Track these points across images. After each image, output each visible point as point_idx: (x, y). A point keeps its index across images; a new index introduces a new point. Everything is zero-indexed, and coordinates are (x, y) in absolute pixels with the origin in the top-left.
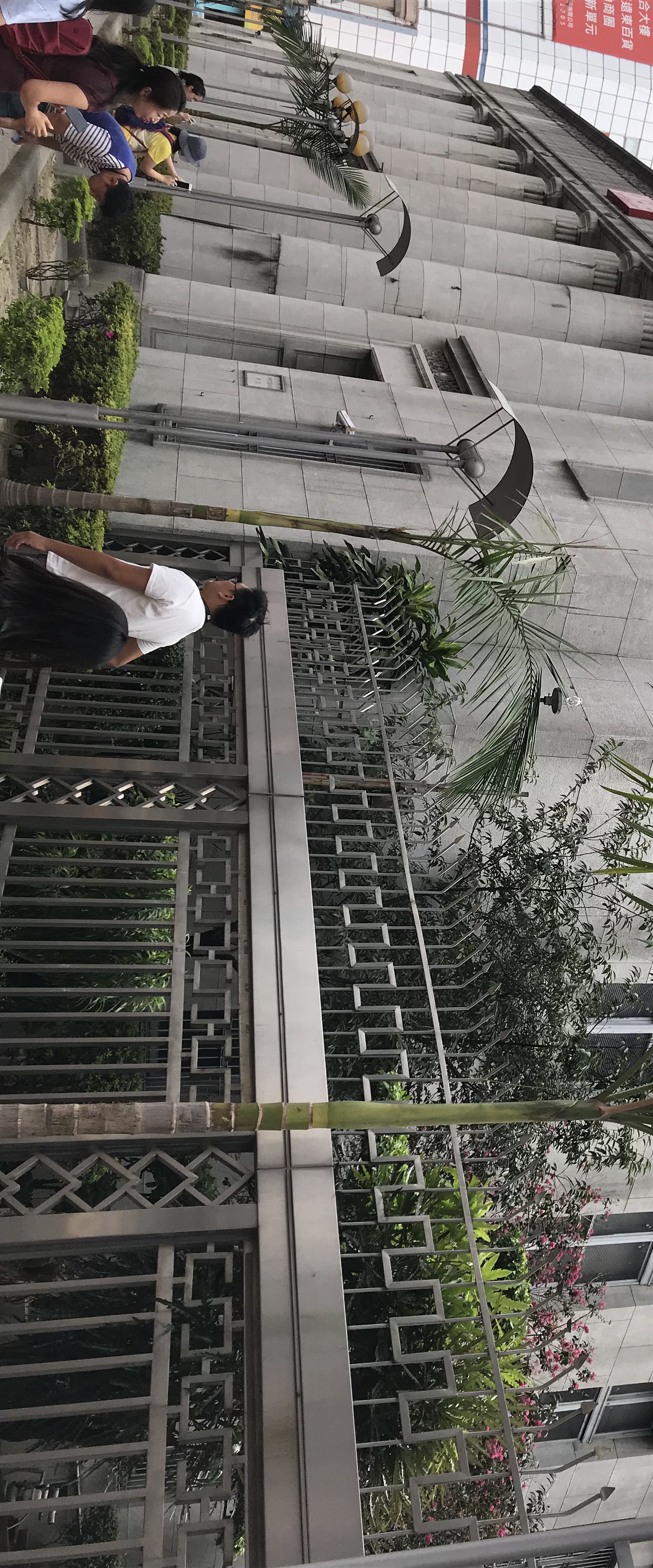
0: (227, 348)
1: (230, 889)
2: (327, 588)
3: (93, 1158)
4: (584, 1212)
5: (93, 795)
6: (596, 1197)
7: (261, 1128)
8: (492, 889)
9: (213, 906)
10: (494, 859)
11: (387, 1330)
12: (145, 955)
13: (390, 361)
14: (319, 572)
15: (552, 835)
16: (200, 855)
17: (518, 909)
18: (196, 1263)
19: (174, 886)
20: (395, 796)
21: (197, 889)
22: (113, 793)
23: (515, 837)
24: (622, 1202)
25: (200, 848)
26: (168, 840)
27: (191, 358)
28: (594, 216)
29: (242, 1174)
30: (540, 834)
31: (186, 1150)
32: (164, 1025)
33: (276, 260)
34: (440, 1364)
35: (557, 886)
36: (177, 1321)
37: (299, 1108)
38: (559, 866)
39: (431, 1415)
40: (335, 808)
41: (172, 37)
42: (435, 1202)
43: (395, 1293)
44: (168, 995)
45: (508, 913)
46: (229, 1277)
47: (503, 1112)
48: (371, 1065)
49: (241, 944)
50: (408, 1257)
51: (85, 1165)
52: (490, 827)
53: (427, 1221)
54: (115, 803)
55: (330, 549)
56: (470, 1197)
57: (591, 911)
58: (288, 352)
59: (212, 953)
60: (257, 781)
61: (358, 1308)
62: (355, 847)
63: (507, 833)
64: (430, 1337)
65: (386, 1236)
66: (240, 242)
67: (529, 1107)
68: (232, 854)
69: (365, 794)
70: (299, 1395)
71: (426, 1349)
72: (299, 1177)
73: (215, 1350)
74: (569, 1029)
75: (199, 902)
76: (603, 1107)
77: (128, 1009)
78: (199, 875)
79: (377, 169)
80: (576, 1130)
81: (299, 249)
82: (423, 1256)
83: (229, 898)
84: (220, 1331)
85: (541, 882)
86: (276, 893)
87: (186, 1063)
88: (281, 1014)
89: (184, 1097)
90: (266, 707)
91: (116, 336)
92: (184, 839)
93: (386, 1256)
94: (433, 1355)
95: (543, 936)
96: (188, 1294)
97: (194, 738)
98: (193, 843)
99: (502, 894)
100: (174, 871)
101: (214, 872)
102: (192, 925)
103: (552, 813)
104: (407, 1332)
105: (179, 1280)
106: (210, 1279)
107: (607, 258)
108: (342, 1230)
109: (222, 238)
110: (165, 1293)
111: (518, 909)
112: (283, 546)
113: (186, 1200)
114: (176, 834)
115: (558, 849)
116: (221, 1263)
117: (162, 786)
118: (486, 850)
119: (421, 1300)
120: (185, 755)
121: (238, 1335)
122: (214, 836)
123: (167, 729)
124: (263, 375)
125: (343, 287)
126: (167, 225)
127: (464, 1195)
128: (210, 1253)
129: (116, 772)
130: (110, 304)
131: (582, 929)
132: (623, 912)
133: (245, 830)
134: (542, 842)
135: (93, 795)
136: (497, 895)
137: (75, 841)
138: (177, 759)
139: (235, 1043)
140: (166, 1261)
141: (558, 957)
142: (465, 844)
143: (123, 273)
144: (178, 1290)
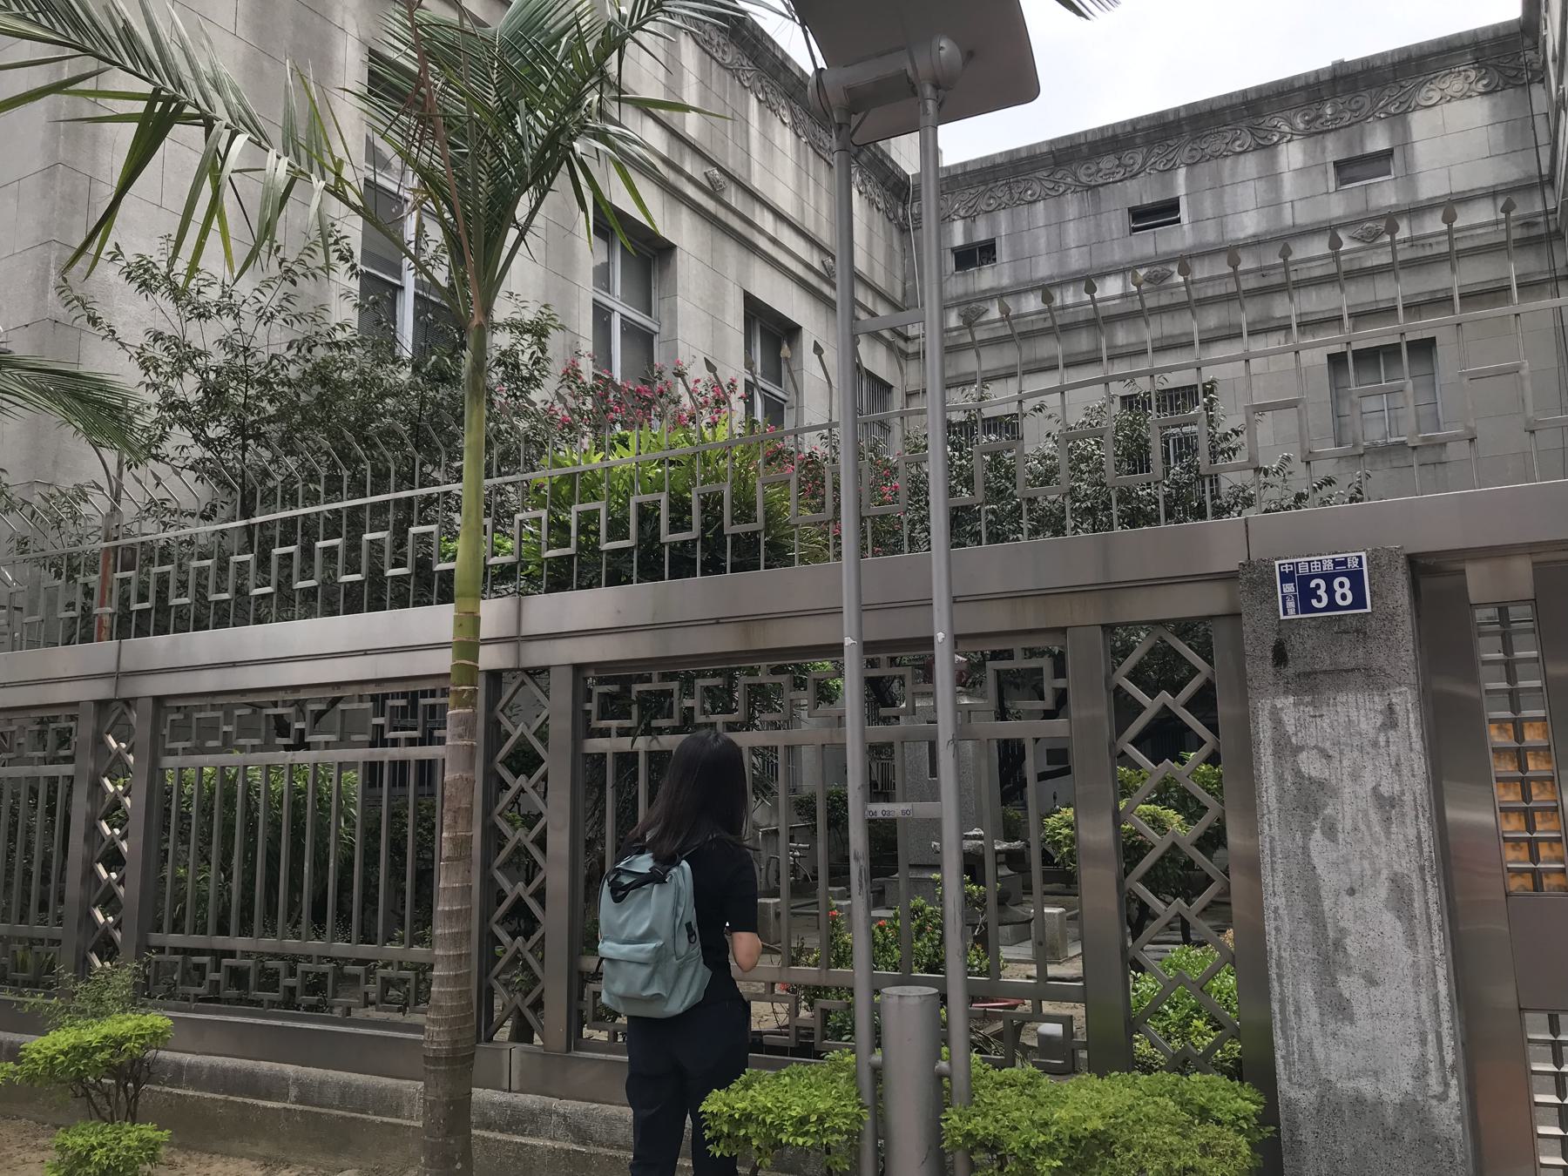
1: (228, 710)
3: (498, 820)
4: (588, 378)
5: (114, 859)
6: (574, 365)
7: (476, 660)
8: (244, 448)
9: (246, 730)
10: (208, 444)
12: (300, 792)
15: (181, 376)
16: (188, 744)
17: (270, 420)
18: (601, 718)
20: (121, 542)
21: (227, 746)
22: (113, 842)
23: (180, 419)
24: (582, 341)
25: (180, 745)
29: (523, 683)
30: (178, 390)
31: (495, 734)
32: (373, 769)
35: (243, 376)
36: (649, 731)
37: (459, 625)
38: (218, 372)
40: (135, 607)
42: (559, 499)
43: (640, 540)
45: (274, 431)
46: (614, 688)
47: (474, 424)
48: (423, 565)
51: (504, 826)
52: (168, 448)
53: (577, 508)
54: (124, 837)
56: (560, 466)
57: (272, 340)
60: (102, 690)
61: (650, 571)
62: (183, 585)
63: (176, 427)
64: (680, 509)
65: (589, 548)
67: (471, 398)
70: (718, 621)
72: (528, 629)
74: (405, 375)
75: (242, 742)
76: (475, 322)
77: (354, 805)
78: (211, 744)
80: (508, 378)
83: (238, 712)
85: (237, 393)
86: (234, 664)
87: (411, 742)
88: (365, 653)
89: (441, 741)
92: (169, 762)
93: (605, 546)
95: (298, 396)
96: (627, 723)
97: (45, 761)
98: (173, 752)
99: (250, 437)
100: (206, 770)
101: (211, 728)
102: (267, 746)
104: (673, 529)
105: (613, 732)
106: (614, 706)
108: (580, 587)
110: (625, 744)
111: (270, 420)
115: (197, 371)
117: (105, 791)
118: (197, 452)
119: (647, 515)
120: (68, 769)
121: (665, 677)
122: (166, 732)
123: (34, 793)
127: (557, 473)
128: (592, 707)
129: (86, 839)
131: (294, 351)
132: (275, 303)
133: (159, 700)
134: (188, 388)
135: (114, 859)
136: (251, 441)
138: (71, 778)
139: (395, 696)
140: (596, 745)
141: (324, 381)
142: (189, 476)
144: (623, 732)
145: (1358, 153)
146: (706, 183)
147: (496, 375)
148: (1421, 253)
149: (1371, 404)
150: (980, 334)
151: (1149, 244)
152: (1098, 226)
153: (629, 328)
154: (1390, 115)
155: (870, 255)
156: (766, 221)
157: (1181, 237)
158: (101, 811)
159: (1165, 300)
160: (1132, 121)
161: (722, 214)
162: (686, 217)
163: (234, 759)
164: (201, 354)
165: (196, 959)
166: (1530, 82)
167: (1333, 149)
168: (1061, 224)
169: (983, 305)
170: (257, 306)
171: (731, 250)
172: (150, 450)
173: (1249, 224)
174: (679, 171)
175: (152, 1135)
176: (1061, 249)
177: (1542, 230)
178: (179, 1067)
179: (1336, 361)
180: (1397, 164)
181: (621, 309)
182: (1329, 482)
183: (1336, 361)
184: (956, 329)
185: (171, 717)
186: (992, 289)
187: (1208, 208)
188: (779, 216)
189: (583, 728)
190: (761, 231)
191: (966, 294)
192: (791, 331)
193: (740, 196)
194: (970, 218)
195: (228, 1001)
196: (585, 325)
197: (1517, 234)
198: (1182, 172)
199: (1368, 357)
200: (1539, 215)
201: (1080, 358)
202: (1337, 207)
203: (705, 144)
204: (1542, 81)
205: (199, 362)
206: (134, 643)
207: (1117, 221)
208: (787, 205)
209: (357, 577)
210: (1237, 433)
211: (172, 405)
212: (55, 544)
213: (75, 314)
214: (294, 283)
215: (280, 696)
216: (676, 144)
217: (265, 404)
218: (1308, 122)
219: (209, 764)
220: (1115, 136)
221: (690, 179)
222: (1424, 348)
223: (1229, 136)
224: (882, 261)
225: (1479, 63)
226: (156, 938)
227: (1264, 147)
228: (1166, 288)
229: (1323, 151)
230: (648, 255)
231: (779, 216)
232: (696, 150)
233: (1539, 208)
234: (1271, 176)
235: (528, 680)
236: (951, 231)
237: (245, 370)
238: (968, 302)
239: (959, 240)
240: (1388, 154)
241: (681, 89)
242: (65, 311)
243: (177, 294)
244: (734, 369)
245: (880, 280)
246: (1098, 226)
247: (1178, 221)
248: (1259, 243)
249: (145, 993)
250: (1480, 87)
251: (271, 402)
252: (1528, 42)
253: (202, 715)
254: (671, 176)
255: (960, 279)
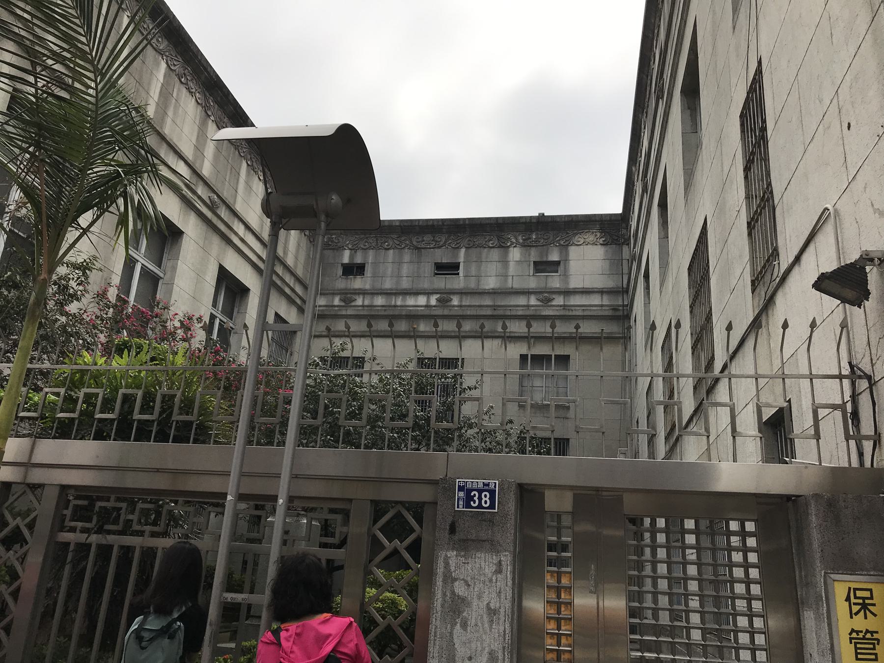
11: (139, 421)
18: (72, 520)
29: (25, 492)
34: (164, 396)
36: (100, 530)
39: (187, 406)
43: (120, 414)
46: (85, 503)
50: (103, 403)
61: (123, 434)
65: (88, 415)
70: (158, 470)
71: (154, 402)
72: (36, 459)
73: (123, 512)
82: (104, 395)
84: (114, 509)
93: (98, 416)
94: (158, 399)
96: (87, 525)
106: (82, 514)
110: (82, 538)
113: (31, 526)
116: (76, 506)
121: (118, 500)
128: (68, 512)
144: (84, 531)
145: (545, 259)
146: (208, 202)
147: (52, 289)
148: (567, 313)
149: (537, 383)
150: (350, 312)
151: (441, 282)
152: (418, 268)
153: (145, 271)
154: (560, 245)
155: (296, 258)
156: (240, 229)
157: (459, 282)
159: (446, 312)
160: (442, 220)
161: (215, 220)
162: (193, 218)
166: (623, 244)
167: (534, 255)
168: (400, 263)
169: (354, 297)
171: (216, 240)
173: (491, 283)
174: (194, 192)
176: (399, 276)
177: (621, 313)
179: (523, 357)
180: (561, 268)
181: (142, 260)
182: (511, 422)
183: (523, 357)
184: (338, 306)
186: (360, 289)
187: (473, 271)
188: (248, 227)
189: (59, 524)
190: (236, 234)
191: (346, 289)
192: (244, 291)
193: (227, 213)
194: (354, 250)
196: (118, 267)
197: (610, 313)
198: (463, 250)
199: (540, 360)
200: (620, 306)
201: (400, 334)
202: (532, 283)
203: (212, 182)
204: (628, 244)
207: (428, 268)
208: (254, 223)
210: (470, 389)
216: (194, 180)
218: (524, 240)
220: (433, 226)
221: (199, 197)
222: (563, 360)
223: (488, 238)
224: (302, 262)
225: (602, 230)
227: (503, 247)
228: (448, 306)
229: (529, 255)
230: (166, 236)
231: (248, 227)
232: (206, 183)
233: (621, 303)
234: (505, 262)
235: (28, 491)
236: (343, 255)
238: (346, 294)
239: (346, 260)
240: (558, 263)
241: (204, 150)
244: (205, 310)
245: (300, 272)
246: (418, 268)
247: (458, 274)
248: (495, 293)
250: (601, 241)
252: (624, 225)
254: (189, 194)
255: (344, 281)
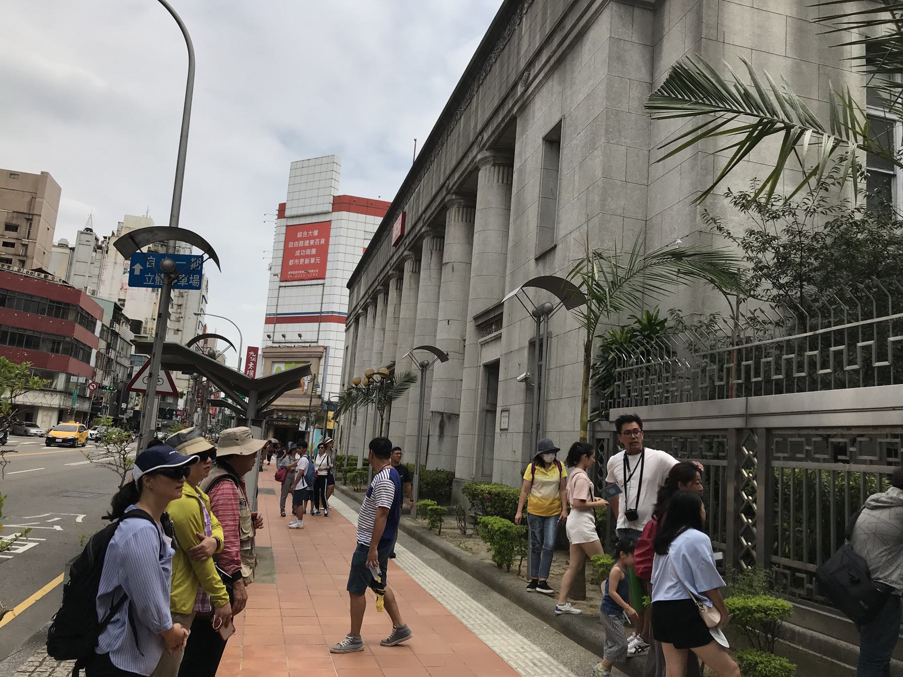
0: (488, 439)
1: (808, 438)
2: (619, 386)
5: (750, 512)
8: (801, 287)
9: (818, 449)
10: (781, 286)
13: (490, 354)
14: (608, 391)
16: (786, 455)
17: (815, 270)
19: (807, 470)
21: (808, 457)
26: (777, 474)
27: (496, 456)
28: (406, 253)
30: (763, 260)
33: (442, 413)
35: (798, 247)
38: (784, 247)
40: (754, 380)
41: (345, 463)
44: (881, 475)
49: (845, 432)
52: (759, 291)
54: (755, 501)
55: (594, 385)
57: (816, 224)
58: (488, 407)
59: (851, 449)
60: (739, 423)
63: (763, 279)
66: (435, 432)
68: (785, 437)
69: (744, 363)
75: (817, 456)
78: (799, 455)
79: (394, 364)
81: (436, 403)
83: (814, 439)
86: (810, 412)
88: (894, 409)
90: (692, 418)
91: (489, 493)
92: (776, 464)
98: (778, 459)
101: (797, 447)
103: (749, 252)
107: (426, 244)
109: (434, 440)
111: (815, 270)
112: (593, 411)
114: (773, 468)
115: (773, 248)
118: (775, 292)
120: (724, 463)
122: (773, 447)
124: (501, 421)
125: (453, 380)
126: (431, 467)
130: (473, 495)
133: (769, 430)
134: (769, 257)
135: (750, 512)
136: (805, 283)
137: (779, 524)
143: (456, 490)
158: (742, 486)
163: (811, 465)
164: (775, 238)
165: (798, 574)
170: (805, 207)
172: (749, 292)
175: (786, 664)
178: (793, 631)
185: (775, 440)
195: (816, 601)
205: (775, 243)
206: (754, 399)
209: (886, 363)
211: (759, 267)
212: (705, 345)
213: (710, 227)
214: (827, 190)
215: (840, 432)
217: (812, 260)
219: (799, 466)
226: (775, 559)
237: (800, 243)
242: (705, 225)
243: (761, 208)
249: (770, 588)
251: (815, 259)
253: (793, 439)
